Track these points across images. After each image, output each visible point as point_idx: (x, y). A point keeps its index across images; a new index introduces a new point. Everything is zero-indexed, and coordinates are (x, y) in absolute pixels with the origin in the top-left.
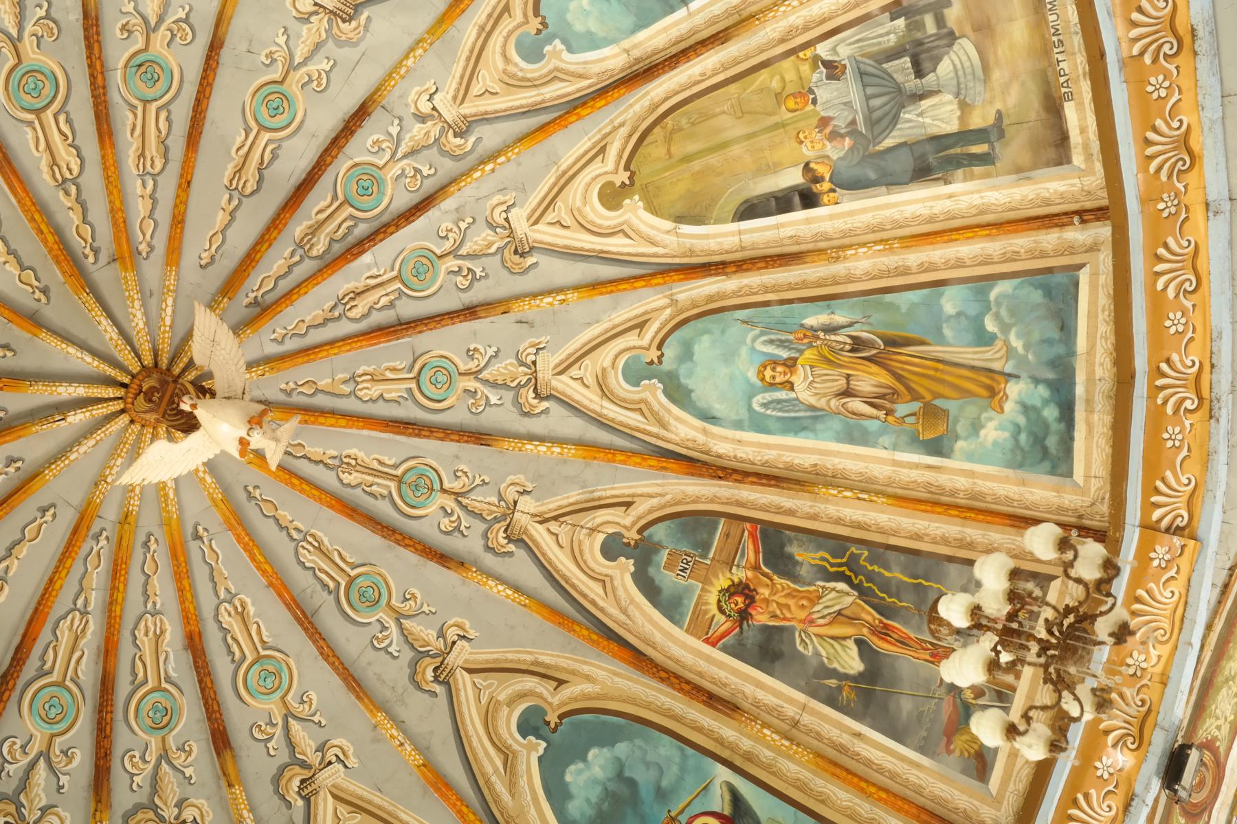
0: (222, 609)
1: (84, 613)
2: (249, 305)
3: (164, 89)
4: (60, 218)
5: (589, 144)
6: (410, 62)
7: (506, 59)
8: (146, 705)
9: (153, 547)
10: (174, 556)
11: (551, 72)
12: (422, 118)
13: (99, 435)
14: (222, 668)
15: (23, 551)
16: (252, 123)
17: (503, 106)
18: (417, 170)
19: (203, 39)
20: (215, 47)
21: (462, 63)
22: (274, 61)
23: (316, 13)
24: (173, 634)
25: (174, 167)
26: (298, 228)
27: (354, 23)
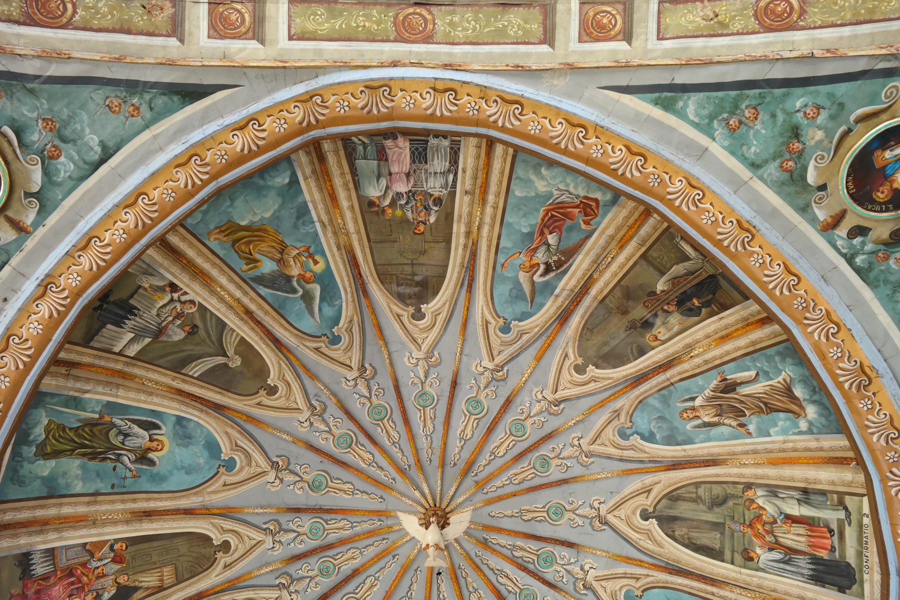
0: (372, 577)
1: (352, 527)
2: (484, 538)
4: (481, 458)
6: (599, 553)
7: (620, 589)
8: (327, 563)
9: (384, 542)
10: (384, 551)
12: (582, 569)
13: (414, 505)
14: (350, 587)
15: (365, 497)
16: (547, 507)
18: (563, 576)
19: (565, 476)
20: (565, 481)
21: (609, 573)
22: (572, 504)
23: (596, 510)
24: (356, 563)
25: (517, 488)
26: (520, 543)
27: (600, 525)
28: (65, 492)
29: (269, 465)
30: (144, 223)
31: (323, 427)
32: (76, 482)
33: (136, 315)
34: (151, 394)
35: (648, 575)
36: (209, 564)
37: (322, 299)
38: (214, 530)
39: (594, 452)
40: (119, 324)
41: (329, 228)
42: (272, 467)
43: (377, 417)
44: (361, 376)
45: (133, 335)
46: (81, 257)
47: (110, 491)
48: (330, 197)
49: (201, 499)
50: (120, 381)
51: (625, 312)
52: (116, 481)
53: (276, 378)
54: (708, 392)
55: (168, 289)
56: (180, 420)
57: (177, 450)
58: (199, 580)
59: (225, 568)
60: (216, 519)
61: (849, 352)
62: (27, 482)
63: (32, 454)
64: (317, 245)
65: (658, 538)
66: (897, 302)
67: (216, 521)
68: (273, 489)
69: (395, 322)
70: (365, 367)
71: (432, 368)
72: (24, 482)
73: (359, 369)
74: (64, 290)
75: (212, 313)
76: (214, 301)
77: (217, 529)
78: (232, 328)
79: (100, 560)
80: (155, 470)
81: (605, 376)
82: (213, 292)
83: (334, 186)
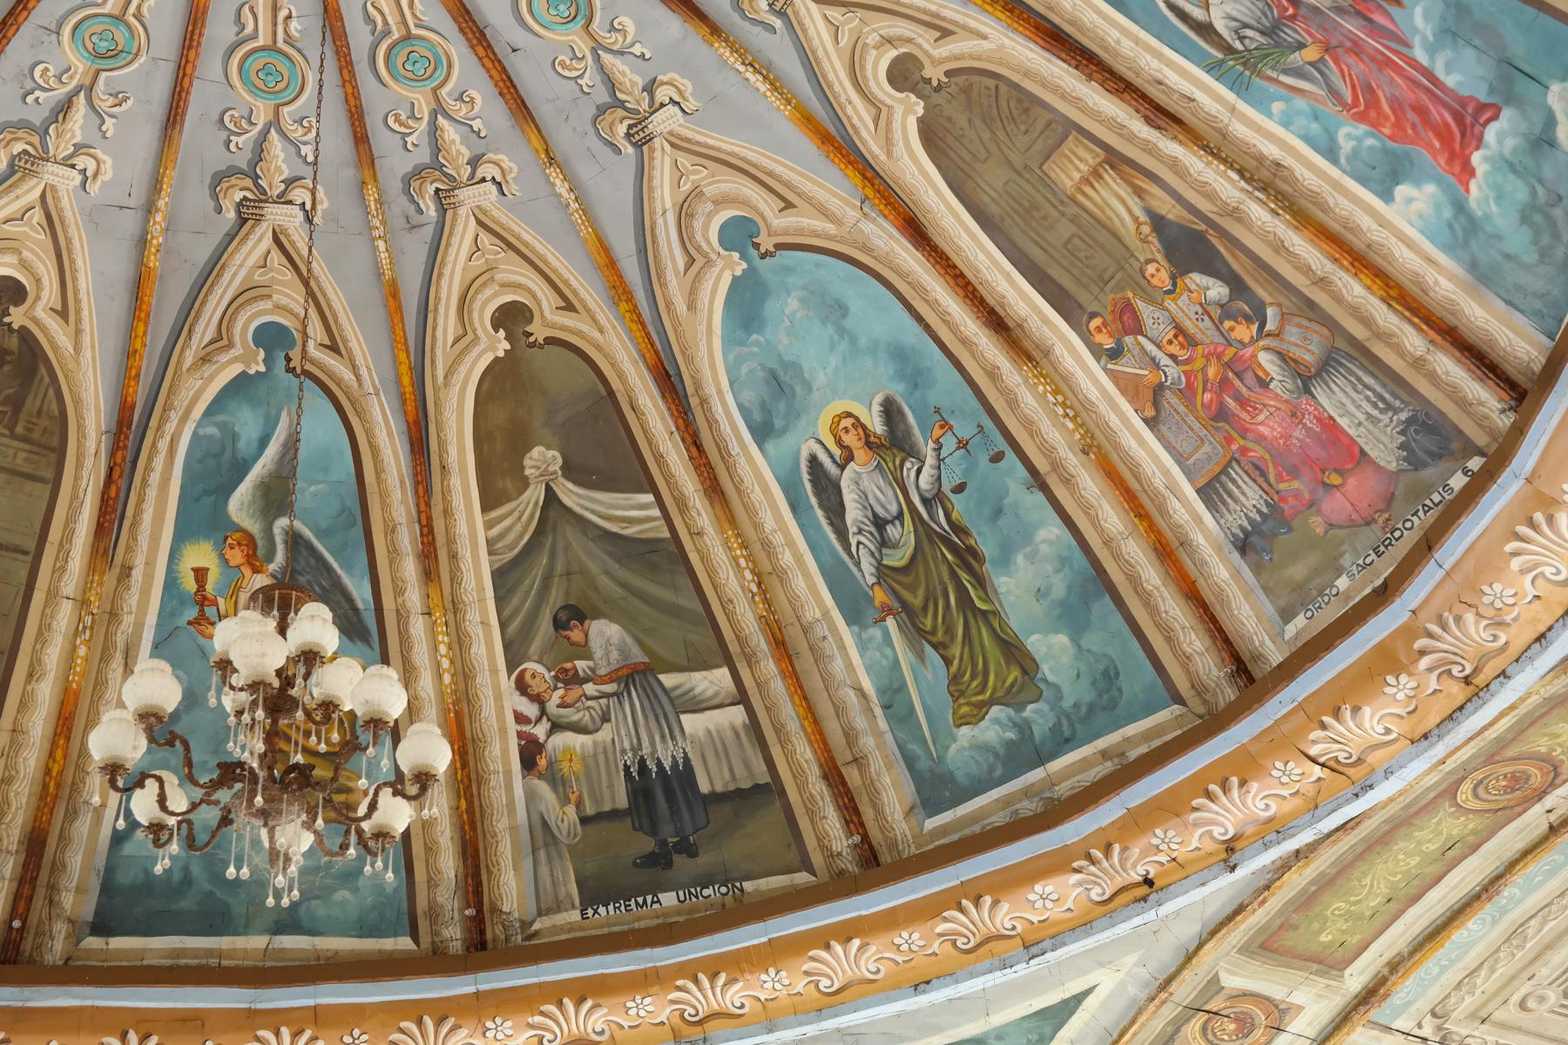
28: (1078, 554)
29: (652, 150)
30: (439, 1022)
31: (450, 132)
32: (1045, 549)
33: (642, 763)
34: (767, 545)
36: (975, 79)
37: (240, 469)
38: (897, 134)
40: (685, 773)
41: (120, 640)
42: (649, 139)
43: (283, 66)
44: (263, 197)
45: (683, 717)
46: (598, 1029)
47: (1010, 455)
48: (70, 730)
49: (867, 227)
50: (794, 634)
52: (983, 459)
53: (482, 346)
55: (542, 762)
56: (763, 432)
57: (821, 379)
58: (1027, 74)
59: (951, 33)
60: (871, 153)
62: (1101, 667)
63: (1042, 705)
64: (173, 615)
67: (876, 150)
68: (688, 86)
69: (83, 295)
70: (239, 213)
71: (37, 122)
72: (1106, 673)
73: (259, 219)
74: (673, 1002)
75: (503, 626)
76: (478, 651)
77: (889, 130)
78: (490, 553)
79: (1154, 363)
80: (897, 390)
82: (464, 674)
83: (47, 746)
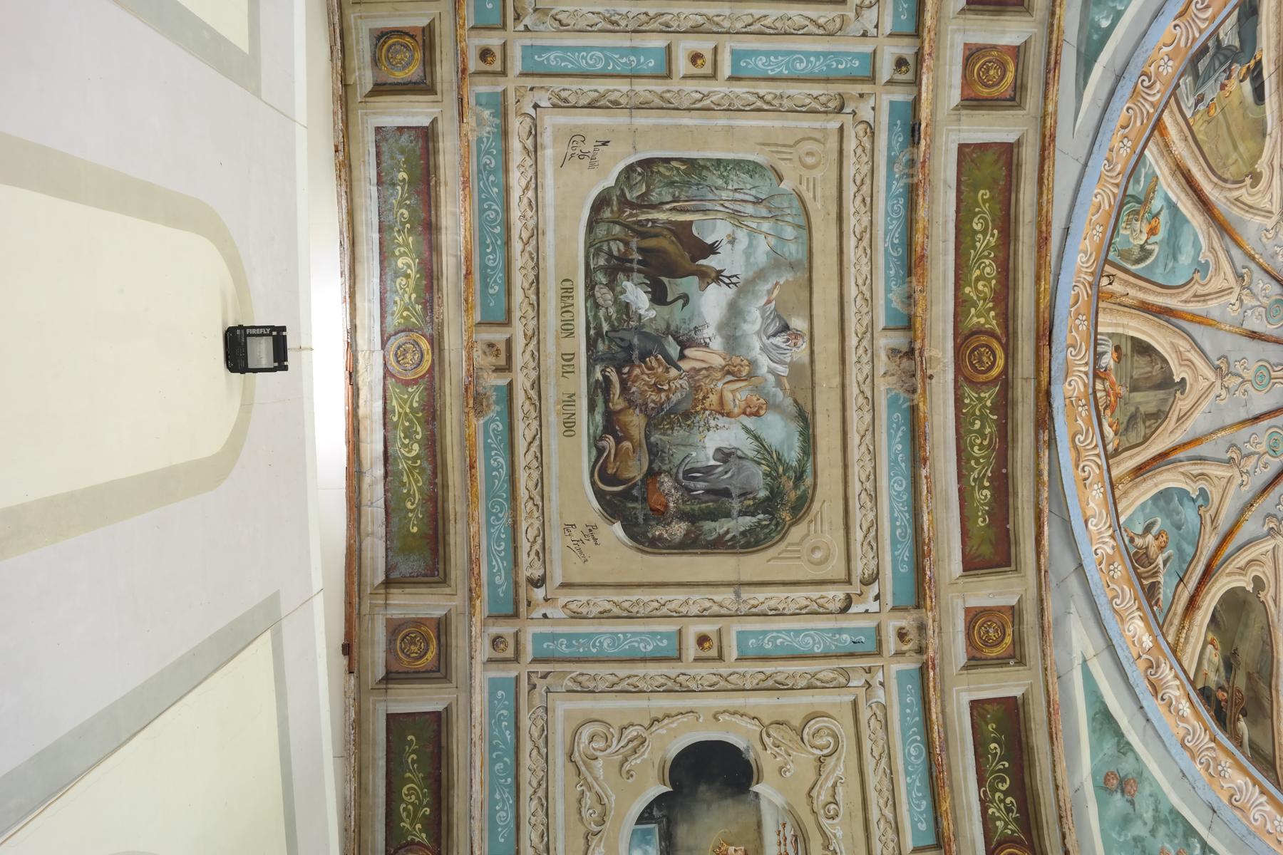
3: (1274, 434)
5: (1235, 209)
11: (1211, 252)
12: (1241, 301)
16: (1271, 384)
17: (1228, 265)
22: (1245, 391)
35: (1185, 302)
39: (1228, 467)
51: (1249, 676)
54: (1161, 579)
61: (1170, 712)
65: (1174, 355)
66: (1151, 795)
81: (1234, 578)
